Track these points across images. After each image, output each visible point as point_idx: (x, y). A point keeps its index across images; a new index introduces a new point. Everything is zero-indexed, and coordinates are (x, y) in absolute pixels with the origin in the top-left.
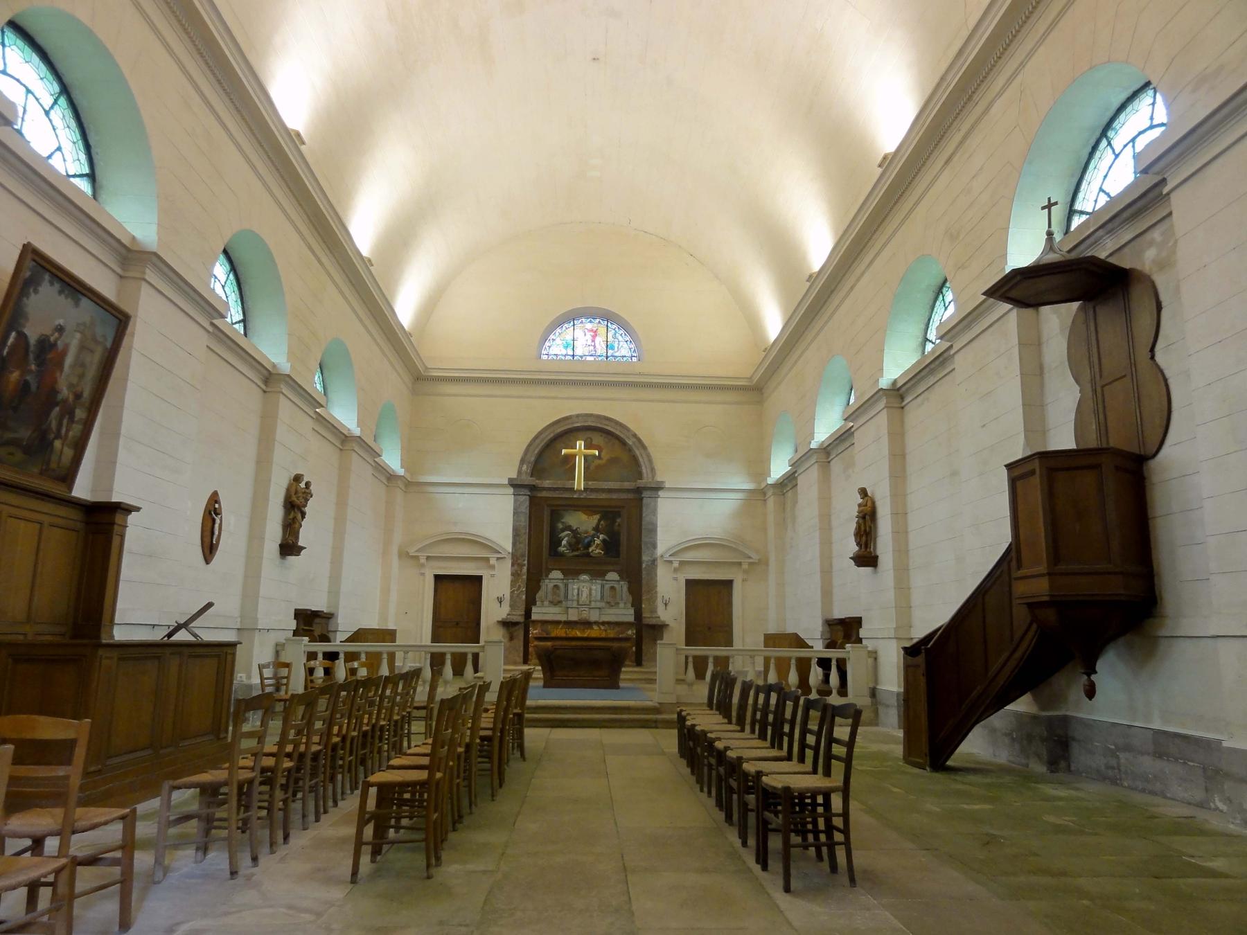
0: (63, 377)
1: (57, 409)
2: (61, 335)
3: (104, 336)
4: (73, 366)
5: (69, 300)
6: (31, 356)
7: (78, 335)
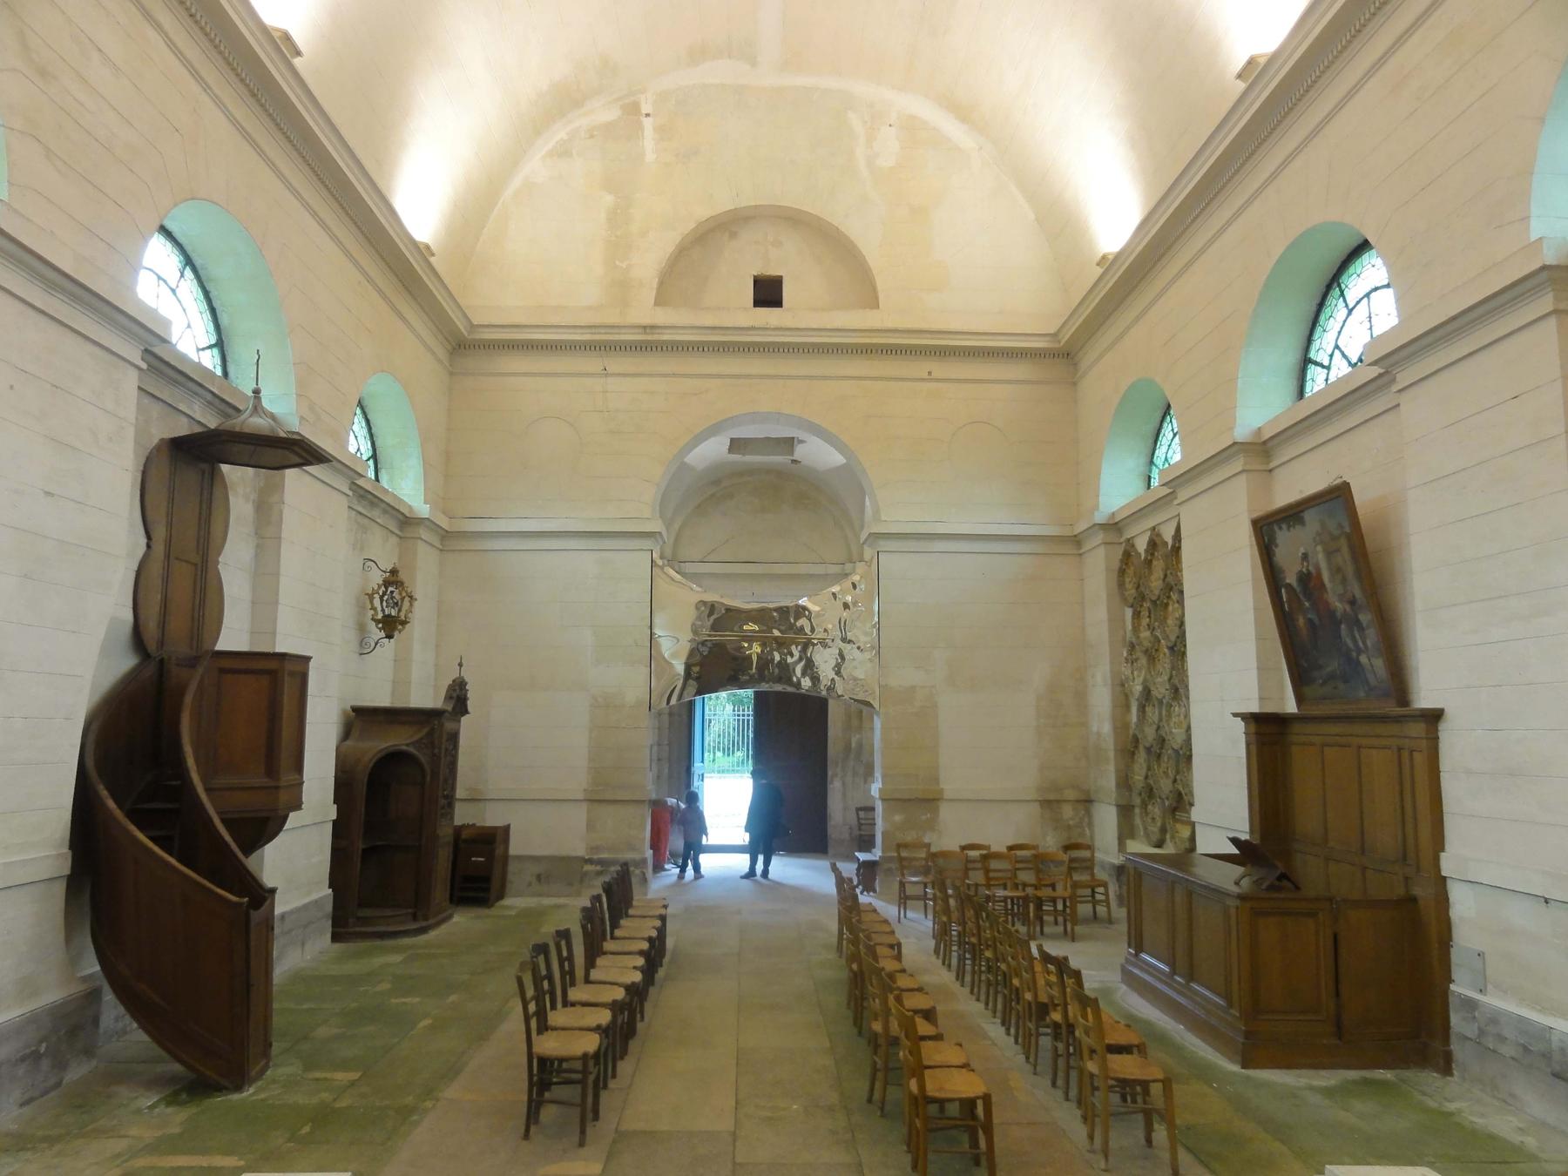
1: (1343, 626)
2: (1308, 562)
3: (1340, 526)
6: (1301, 596)
7: (1319, 548)
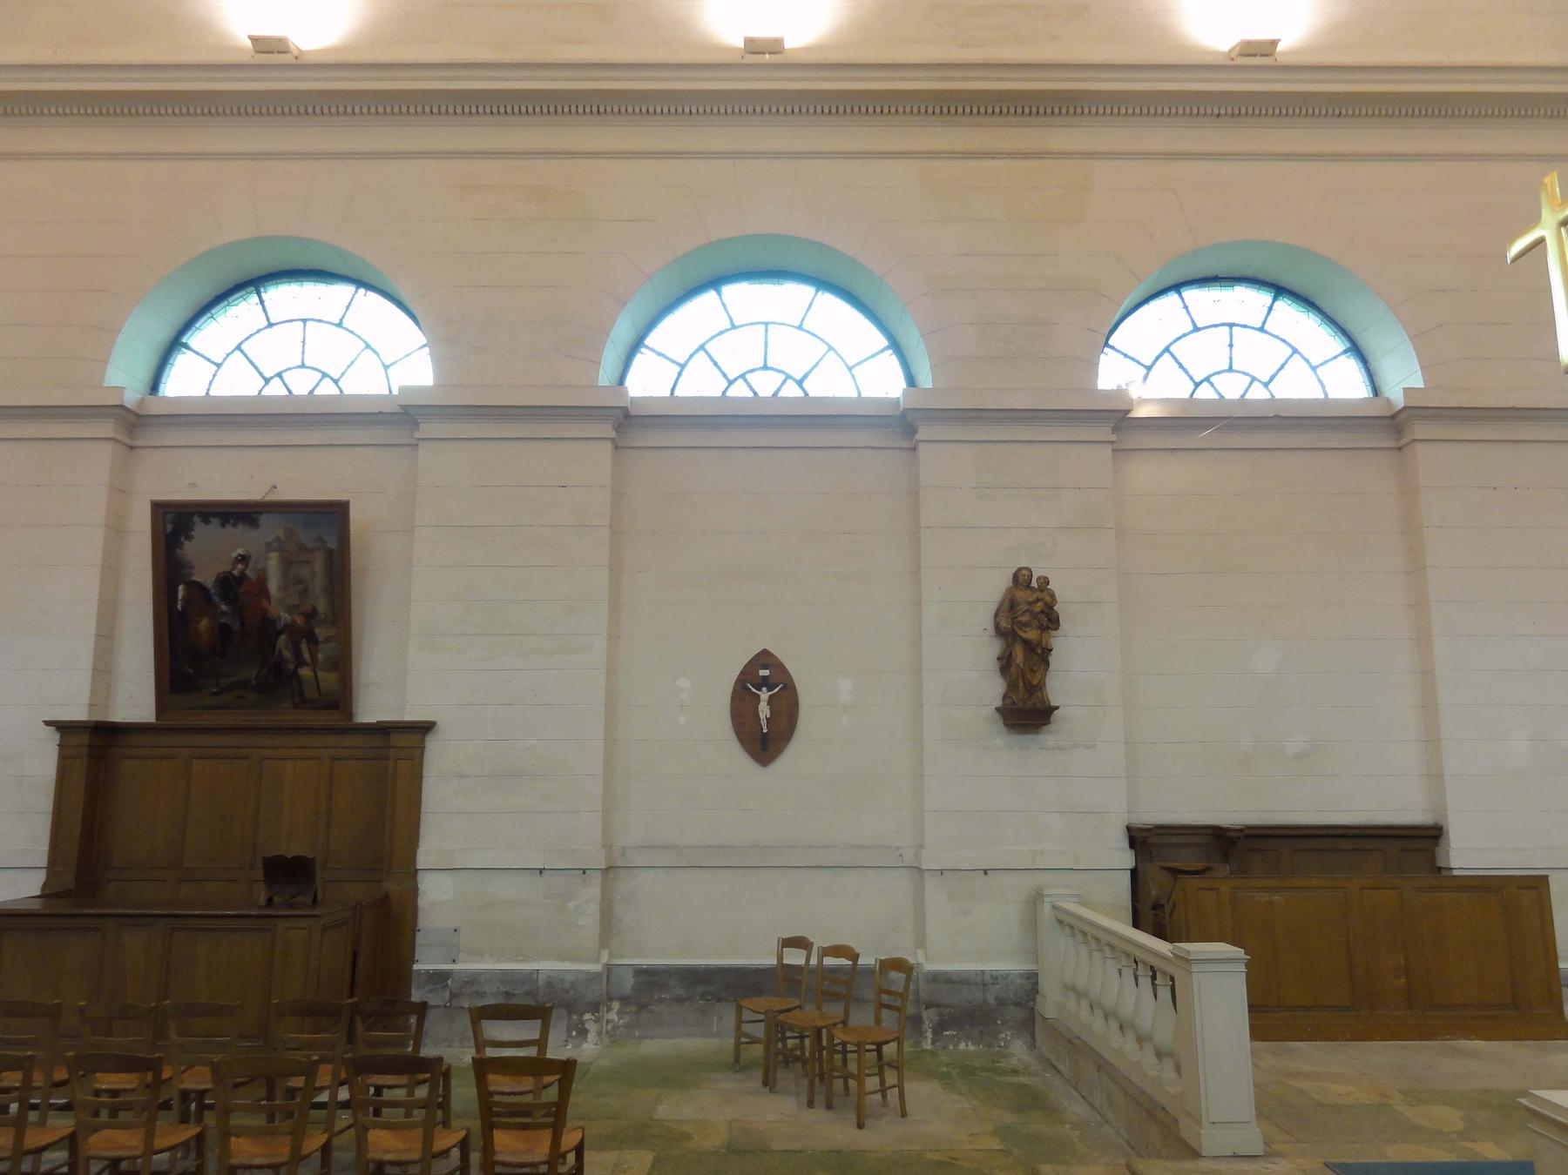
0: (272, 604)
2: (247, 565)
4: (284, 588)
5: (240, 526)
6: (216, 599)
7: (274, 556)
